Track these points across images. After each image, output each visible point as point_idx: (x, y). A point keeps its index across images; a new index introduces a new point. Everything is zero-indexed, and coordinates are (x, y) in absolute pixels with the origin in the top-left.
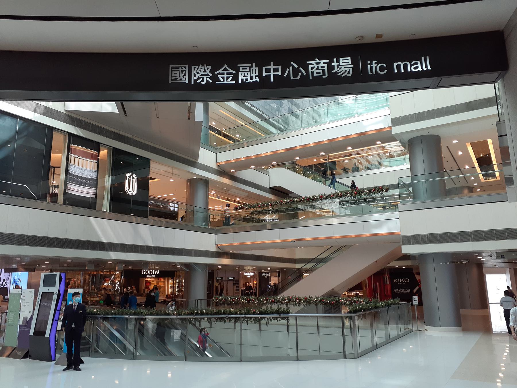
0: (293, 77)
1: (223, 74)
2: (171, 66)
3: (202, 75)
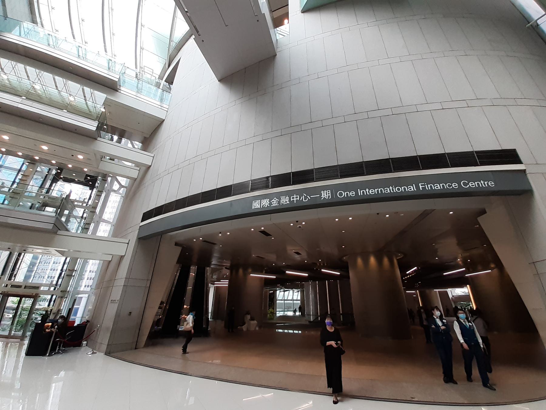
0: (305, 200)
1: (274, 201)
2: (253, 201)
3: (265, 203)
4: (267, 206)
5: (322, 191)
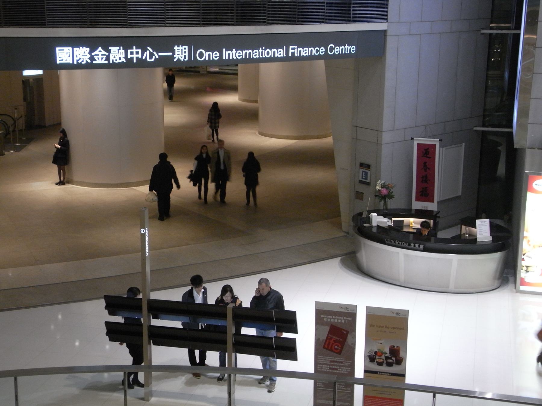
0: (150, 59)
1: (98, 55)
4: (87, 61)
5: (176, 46)
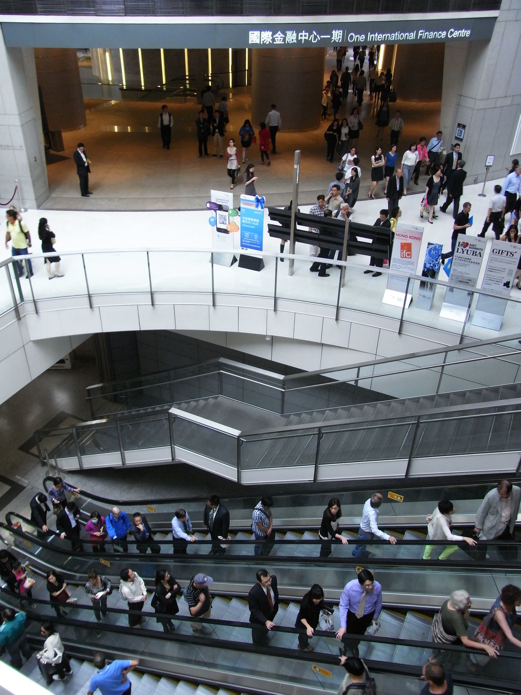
4: (269, 42)
5: (334, 31)
